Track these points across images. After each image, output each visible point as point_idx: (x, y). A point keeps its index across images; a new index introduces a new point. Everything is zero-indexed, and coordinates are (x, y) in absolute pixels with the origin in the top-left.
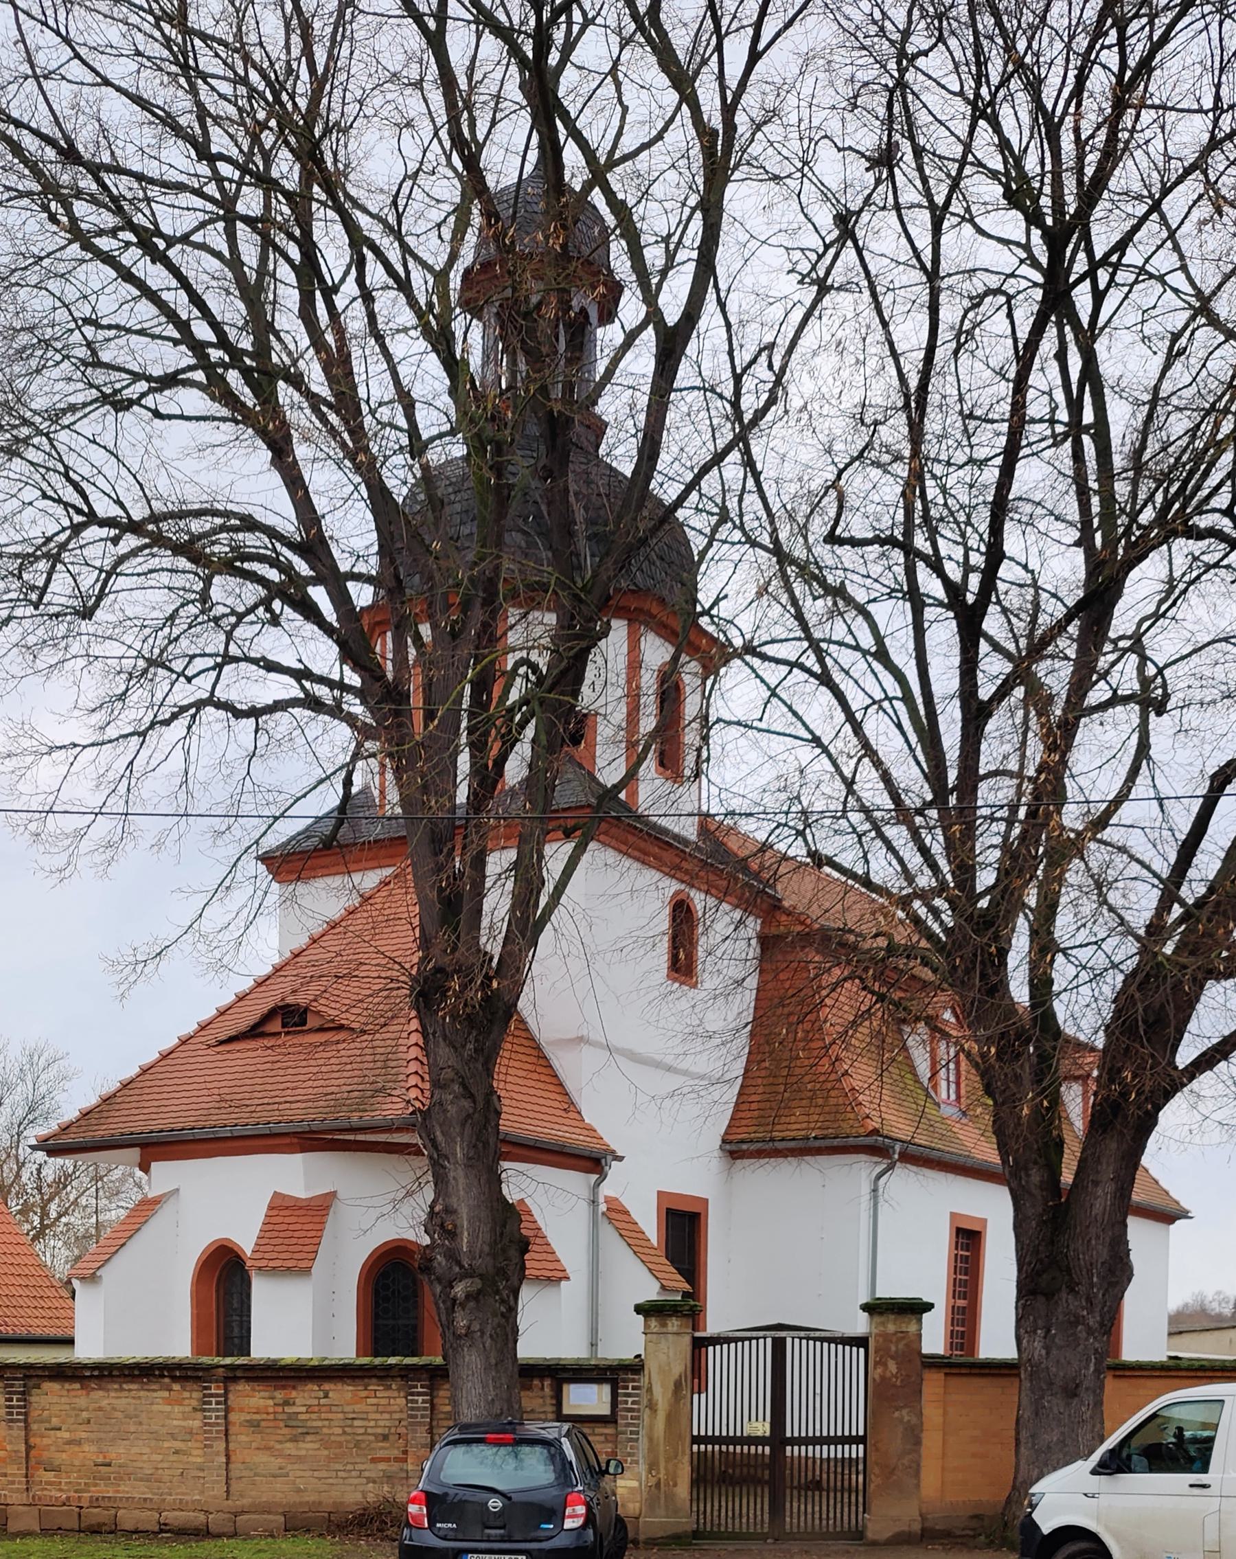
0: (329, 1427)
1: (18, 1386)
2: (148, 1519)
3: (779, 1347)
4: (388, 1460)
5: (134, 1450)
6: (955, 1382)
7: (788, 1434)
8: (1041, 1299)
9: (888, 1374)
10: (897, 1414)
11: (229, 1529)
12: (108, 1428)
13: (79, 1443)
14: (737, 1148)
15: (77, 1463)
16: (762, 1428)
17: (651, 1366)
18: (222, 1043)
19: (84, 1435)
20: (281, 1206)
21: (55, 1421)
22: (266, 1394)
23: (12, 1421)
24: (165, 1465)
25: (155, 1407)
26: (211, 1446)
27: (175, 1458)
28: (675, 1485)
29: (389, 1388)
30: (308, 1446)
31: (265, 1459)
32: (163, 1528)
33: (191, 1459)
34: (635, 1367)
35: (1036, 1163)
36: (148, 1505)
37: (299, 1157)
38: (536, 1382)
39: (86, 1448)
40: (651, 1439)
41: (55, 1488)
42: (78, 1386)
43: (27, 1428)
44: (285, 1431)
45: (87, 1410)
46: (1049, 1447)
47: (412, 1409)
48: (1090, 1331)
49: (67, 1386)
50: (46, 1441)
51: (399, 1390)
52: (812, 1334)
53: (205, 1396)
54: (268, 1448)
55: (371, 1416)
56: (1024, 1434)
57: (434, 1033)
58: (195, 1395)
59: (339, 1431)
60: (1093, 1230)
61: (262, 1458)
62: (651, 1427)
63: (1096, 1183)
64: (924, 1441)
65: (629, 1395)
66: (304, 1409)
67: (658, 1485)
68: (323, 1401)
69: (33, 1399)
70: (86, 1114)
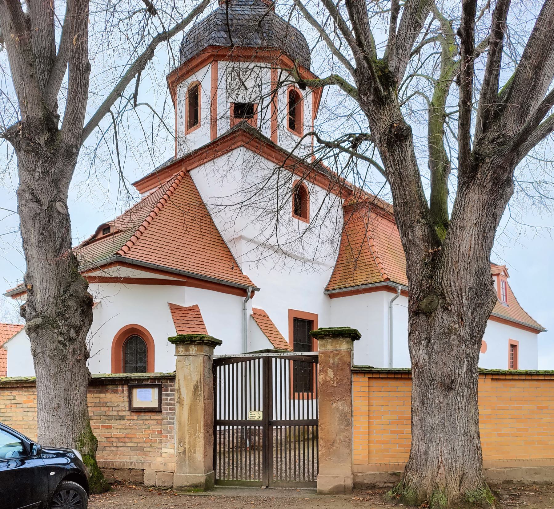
0: (16, 416)
6: (375, 383)
7: (274, 419)
8: (423, 317)
9: (328, 379)
10: (334, 405)
16: (257, 415)
17: (180, 377)
28: (195, 452)
34: (171, 378)
35: (418, 222)
38: (120, 388)
40: (180, 423)
46: (433, 429)
48: (461, 340)
52: (282, 354)
56: (416, 419)
59: (21, 418)
60: (461, 264)
62: (180, 415)
64: (354, 424)
65: (168, 395)
67: (184, 452)
68: (13, 402)
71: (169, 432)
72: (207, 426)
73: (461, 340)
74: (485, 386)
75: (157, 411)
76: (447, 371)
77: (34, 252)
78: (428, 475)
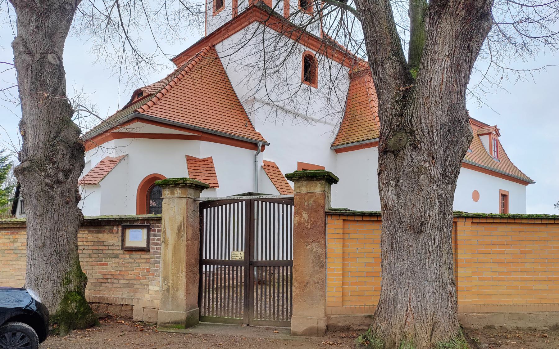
3: (250, 205)
7: (255, 259)
8: (391, 156)
9: (303, 221)
10: (308, 247)
14: (338, 148)
16: (239, 255)
22: (6, 237)
28: (177, 290)
35: (389, 59)
38: (115, 228)
40: (165, 262)
44: (14, 255)
46: (402, 274)
48: (432, 180)
52: (261, 197)
60: (432, 100)
63: (434, 61)
64: (328, 265)
65: (155, 235)
66: (20, 244)
67: (168, 290)
71: (156, 271)
72: (190, 265)
73: (432, 180)
74: (465, 229)
75: (146, 250)
76: (416, 213)
77: (27, 99)
78: (397, 322)
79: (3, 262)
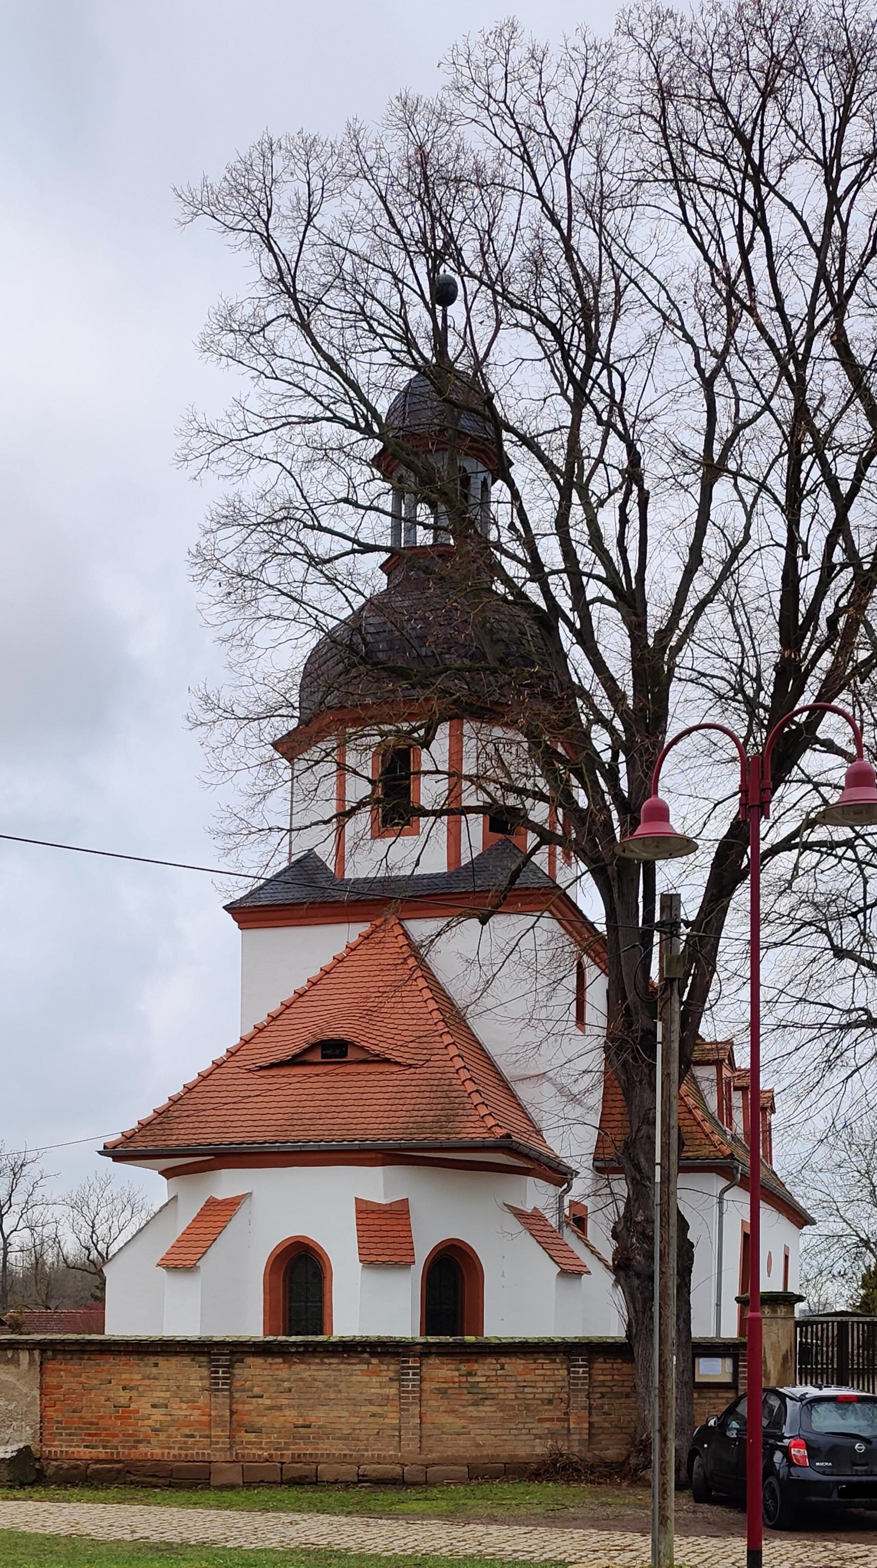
0: (505, 1393)
1: (224, 1360)
2: (348, 1471)
4: (552, 1420)
5: (332, 1414)
11: (421, 1478)
12: (309, 1396)
13: (280, 1408)
15: (277, 1425)
18: (262, 1068)
19: (285, 1402)
20: (366, 1212)
21: (256, 1390)
22: (452, 1367)
23: (218, 1390)
24: (362, 1426)
25: (353, 1378)
26: (408, 1410)
27: (372, 1420)
29: (554, 1361)
30: (487, 1410)
31: (450, 1420)
32: (362, 1479)
33: (387, 1421)
36: (348, 1460)
37: (379, 1170)
39: (287, 1412)
41: (255, 1448)
42: (280, 1360)
43: (231, 1397)
44: (469, 1397)
45: (288, 1380)
47: (574, 1378)
49: (270, 1360)
50: (248, 1407)
51: (562, 1363)
53: (403, 1368)
54: (454, 1411)
55: (539, 1384)
57: (641, 1081)
58: (392, 1367)
59: (513, 1396)
61: (448, 1419)
66: (483, 1379)
68: (499, 1372)
69: (236, 1371)
70: (144, 1126)
79: (442, 1409)
